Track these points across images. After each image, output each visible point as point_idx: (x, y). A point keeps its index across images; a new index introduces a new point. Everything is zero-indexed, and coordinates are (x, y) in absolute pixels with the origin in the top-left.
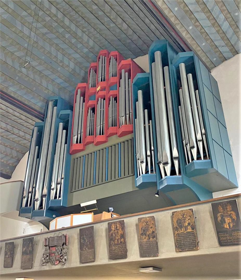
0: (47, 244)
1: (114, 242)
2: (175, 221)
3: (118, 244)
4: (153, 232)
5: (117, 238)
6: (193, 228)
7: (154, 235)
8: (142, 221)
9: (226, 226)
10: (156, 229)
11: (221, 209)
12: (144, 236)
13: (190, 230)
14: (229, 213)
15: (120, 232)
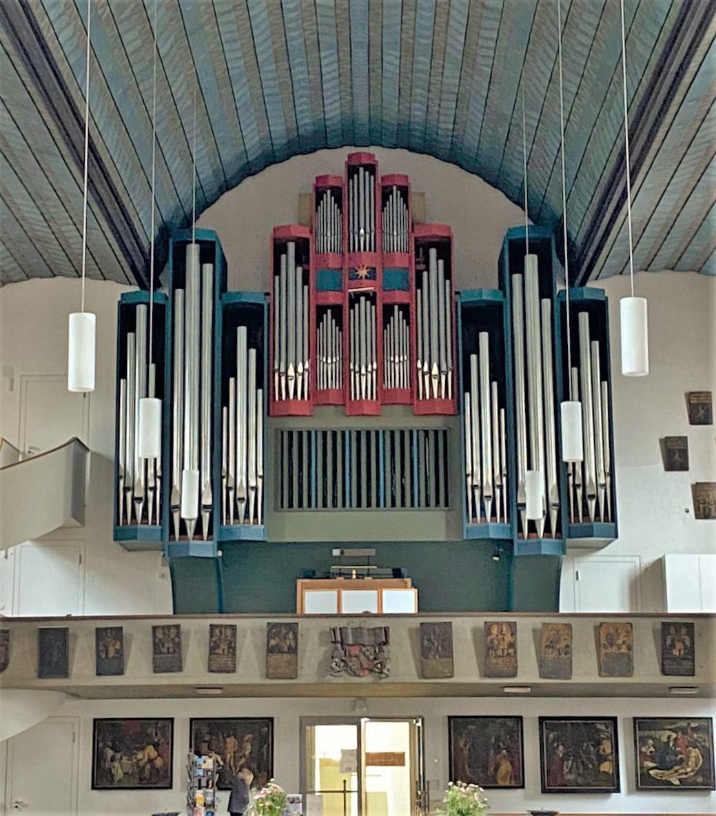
0: (339, 639)
1: (495, 651)
2: (603, 636)
3: (500, 657)
4: (567, 646)
5: (502, 647)
6: (629, 648)
7: (568, 650)
8: (550, 627)
9: (676, 653)
10: (571, 642)
11: (672, 630)
12: (550, 650)
13: (624, 650)
14: (683, 637)
15: (508, 638)
